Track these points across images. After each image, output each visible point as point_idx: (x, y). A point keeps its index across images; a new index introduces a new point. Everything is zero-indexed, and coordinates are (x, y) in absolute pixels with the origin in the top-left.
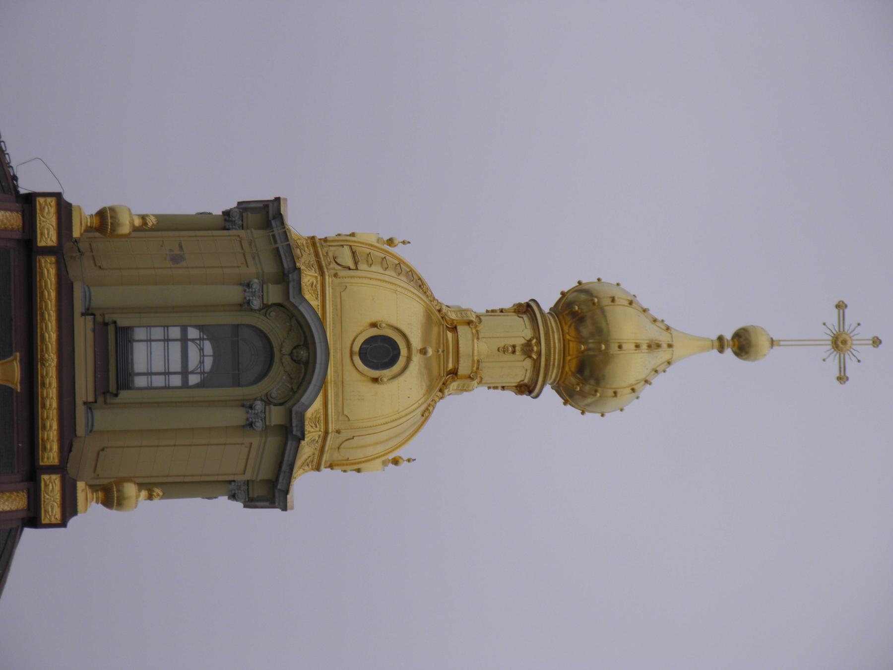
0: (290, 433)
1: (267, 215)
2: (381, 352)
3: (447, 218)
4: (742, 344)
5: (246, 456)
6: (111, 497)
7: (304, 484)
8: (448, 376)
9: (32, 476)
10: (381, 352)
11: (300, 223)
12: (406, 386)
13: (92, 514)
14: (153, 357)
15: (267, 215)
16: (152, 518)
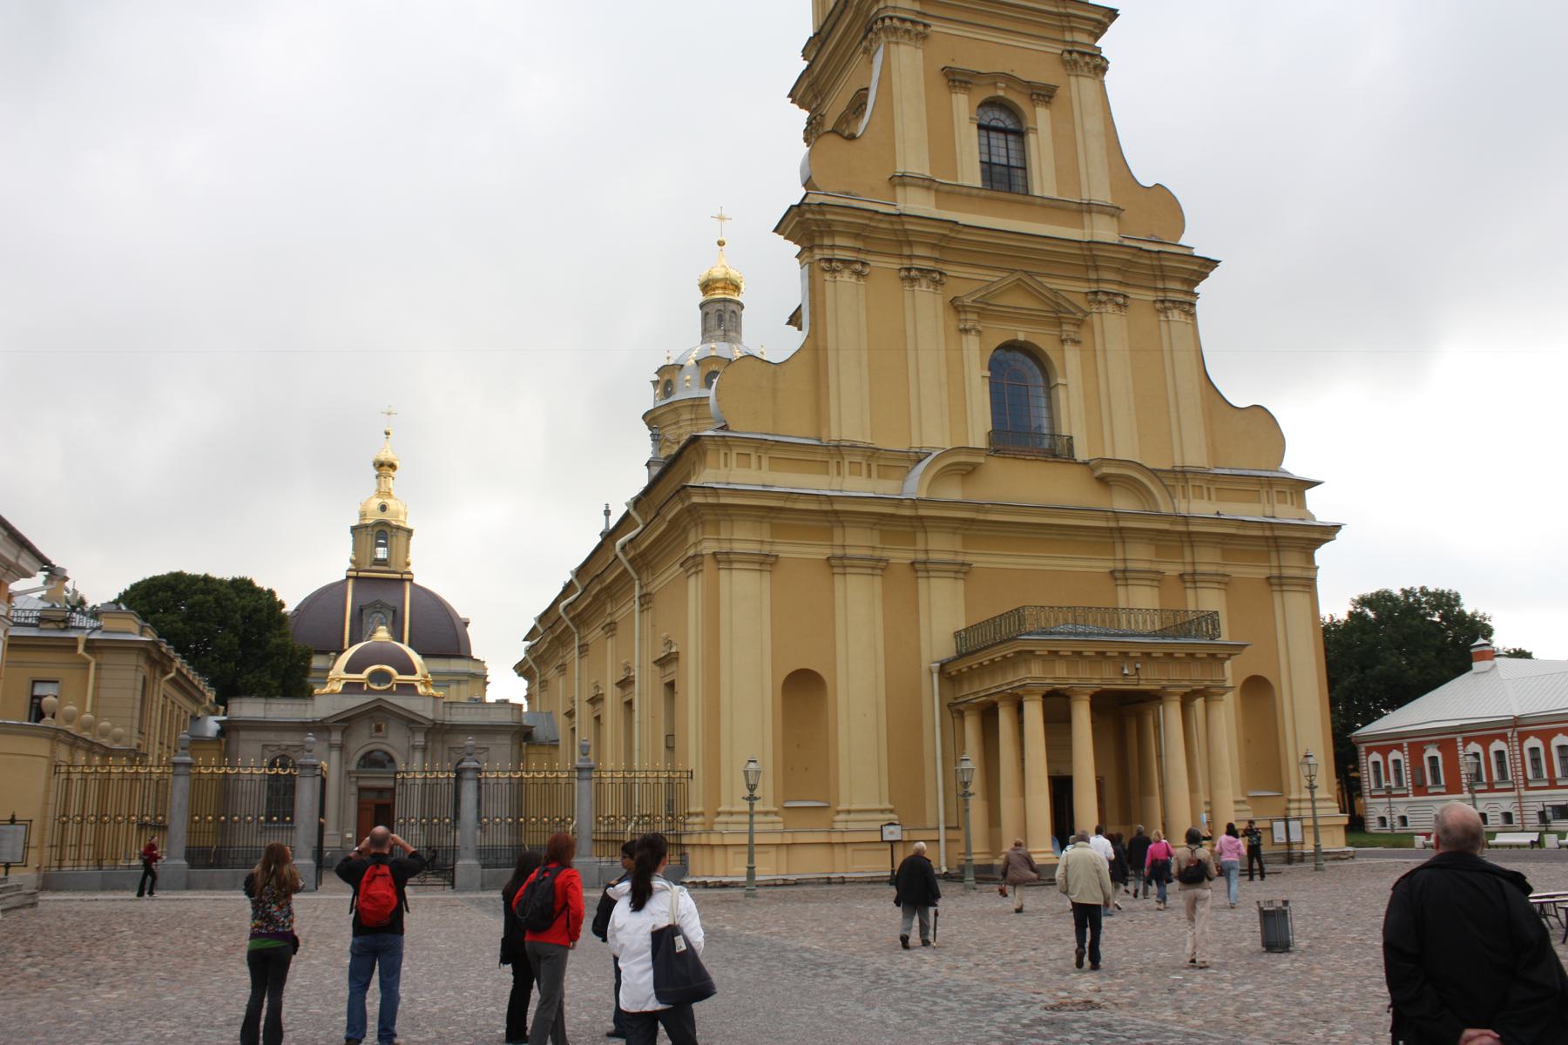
0: (398, 528)
1: (354, 529)
2: (383, 508)
3: (357, 500)
4: (387, 433)
5: (402, 536)
6: (408, 564)
7: (409, 526)
8: (389, 495)
9: (403, 580)
10: (383, 508)
11: (356, 522)
12: (391, 503)
13: (411, 568)
14: (381, 553)
15: (354, 529)
16: (412, 558)
